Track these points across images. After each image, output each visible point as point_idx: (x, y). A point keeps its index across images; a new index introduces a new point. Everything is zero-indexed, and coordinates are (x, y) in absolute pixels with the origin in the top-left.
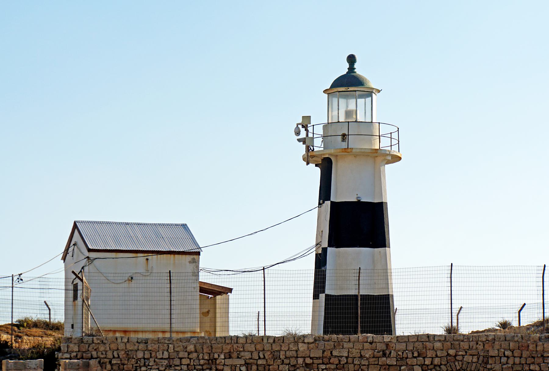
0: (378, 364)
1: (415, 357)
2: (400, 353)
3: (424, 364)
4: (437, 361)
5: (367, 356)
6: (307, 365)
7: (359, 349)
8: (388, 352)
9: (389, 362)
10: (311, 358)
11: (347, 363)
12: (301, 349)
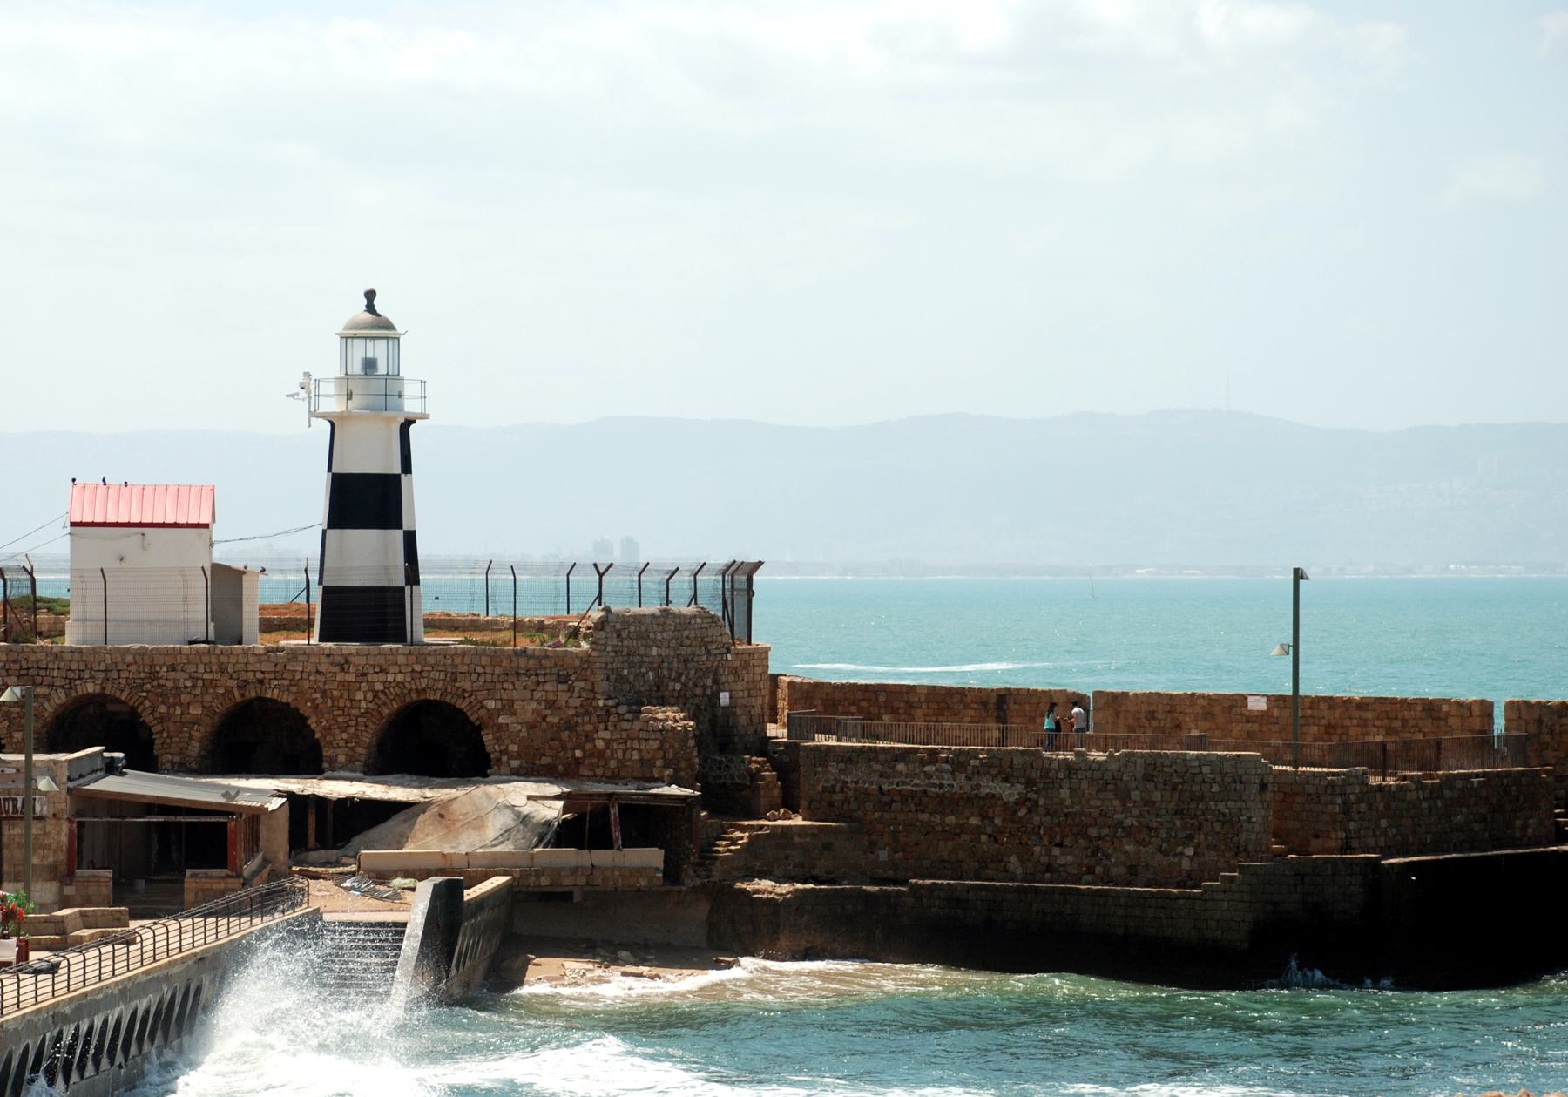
4: (400, 678)
6: (261, 682)
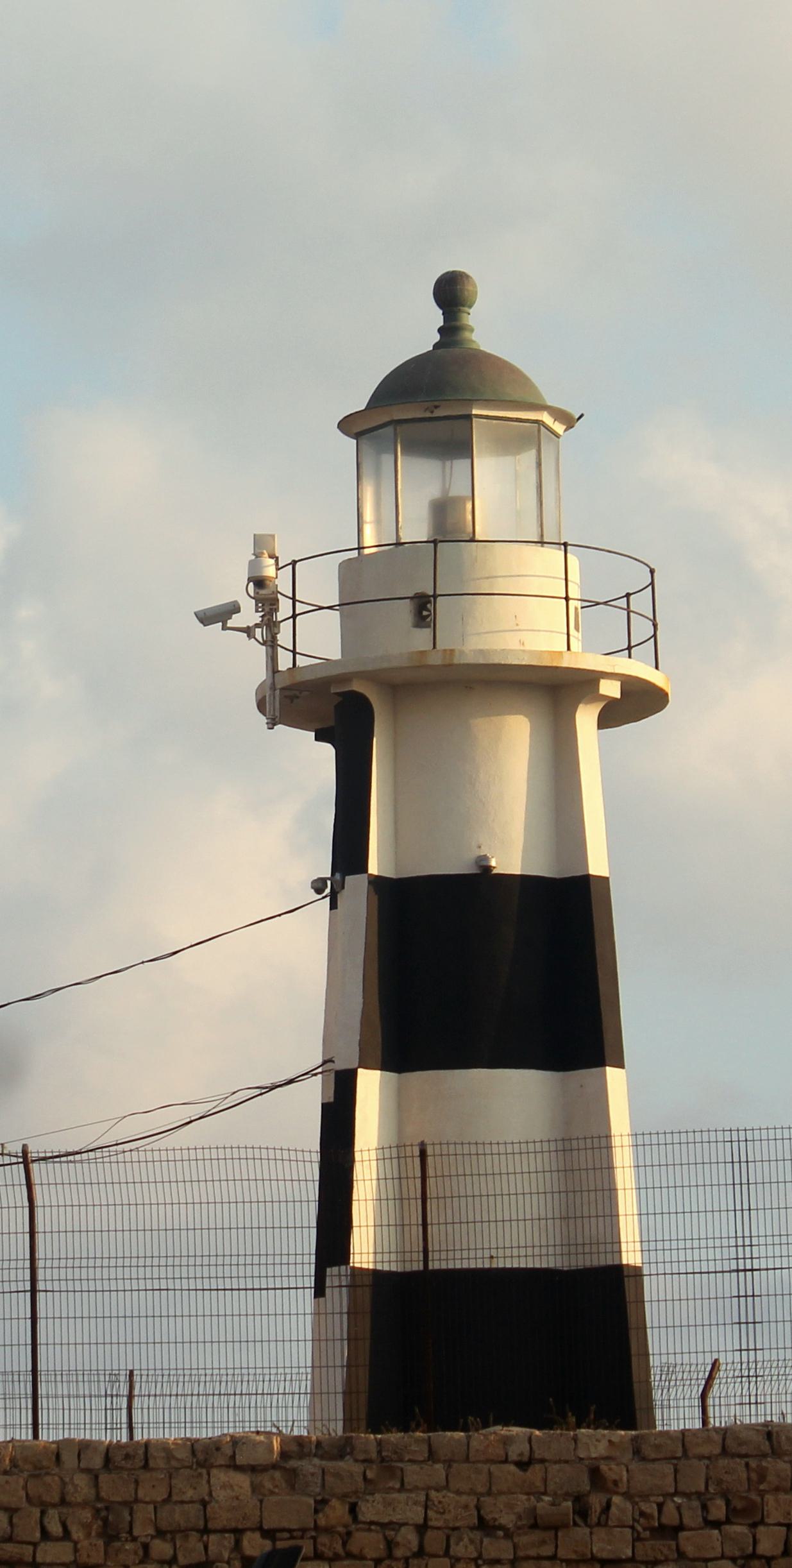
0: (553, 1558)
1: (716, 1524)
2: (651, 1508)
3: (754, 1556)
5: (507, 1520)
7: (472, 1492)
8: (596, 1502)
9: (605, 1544)
10: (269, 1534)
11: (421, 1553)
12: (221, 1495)
